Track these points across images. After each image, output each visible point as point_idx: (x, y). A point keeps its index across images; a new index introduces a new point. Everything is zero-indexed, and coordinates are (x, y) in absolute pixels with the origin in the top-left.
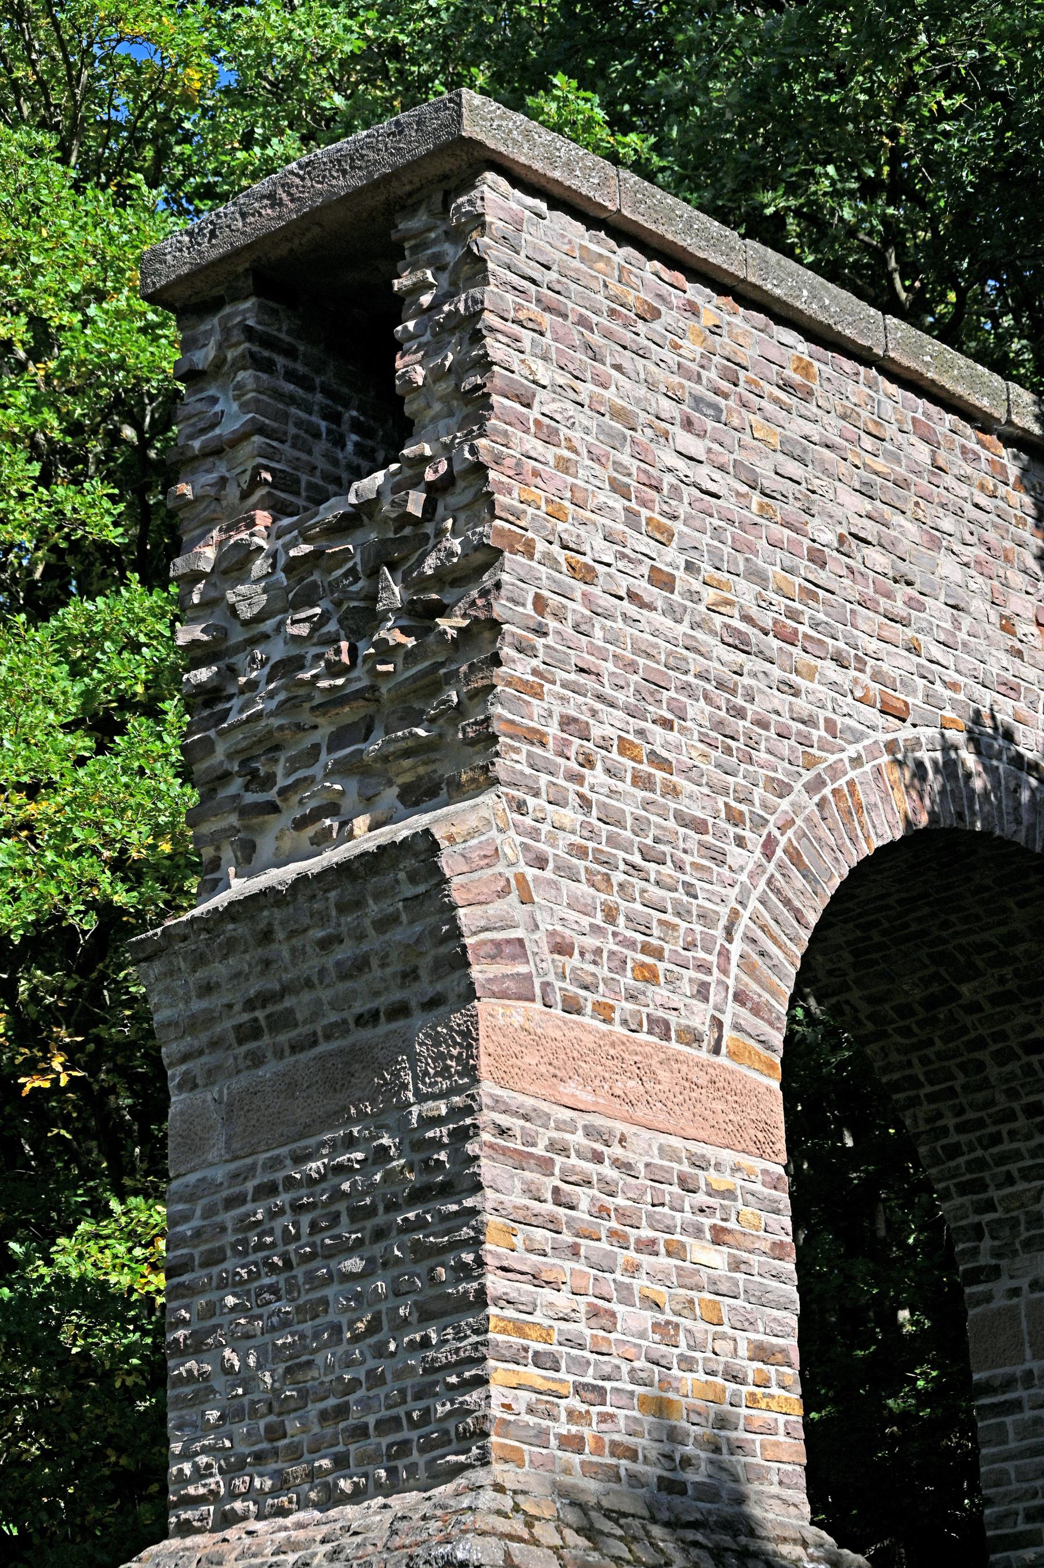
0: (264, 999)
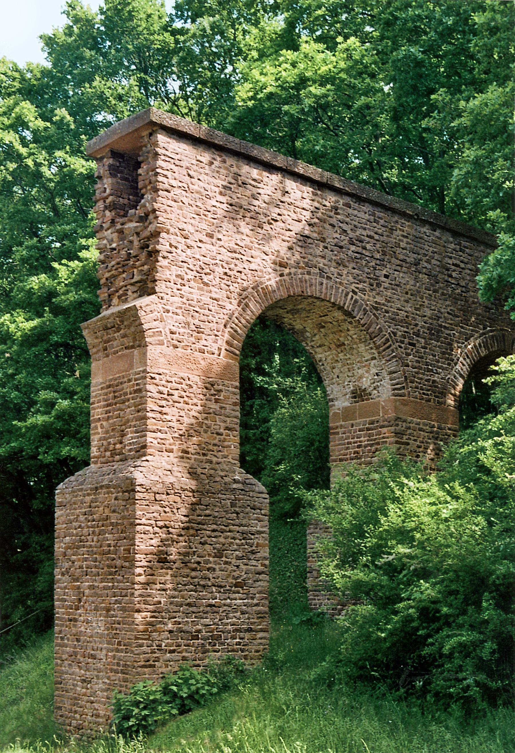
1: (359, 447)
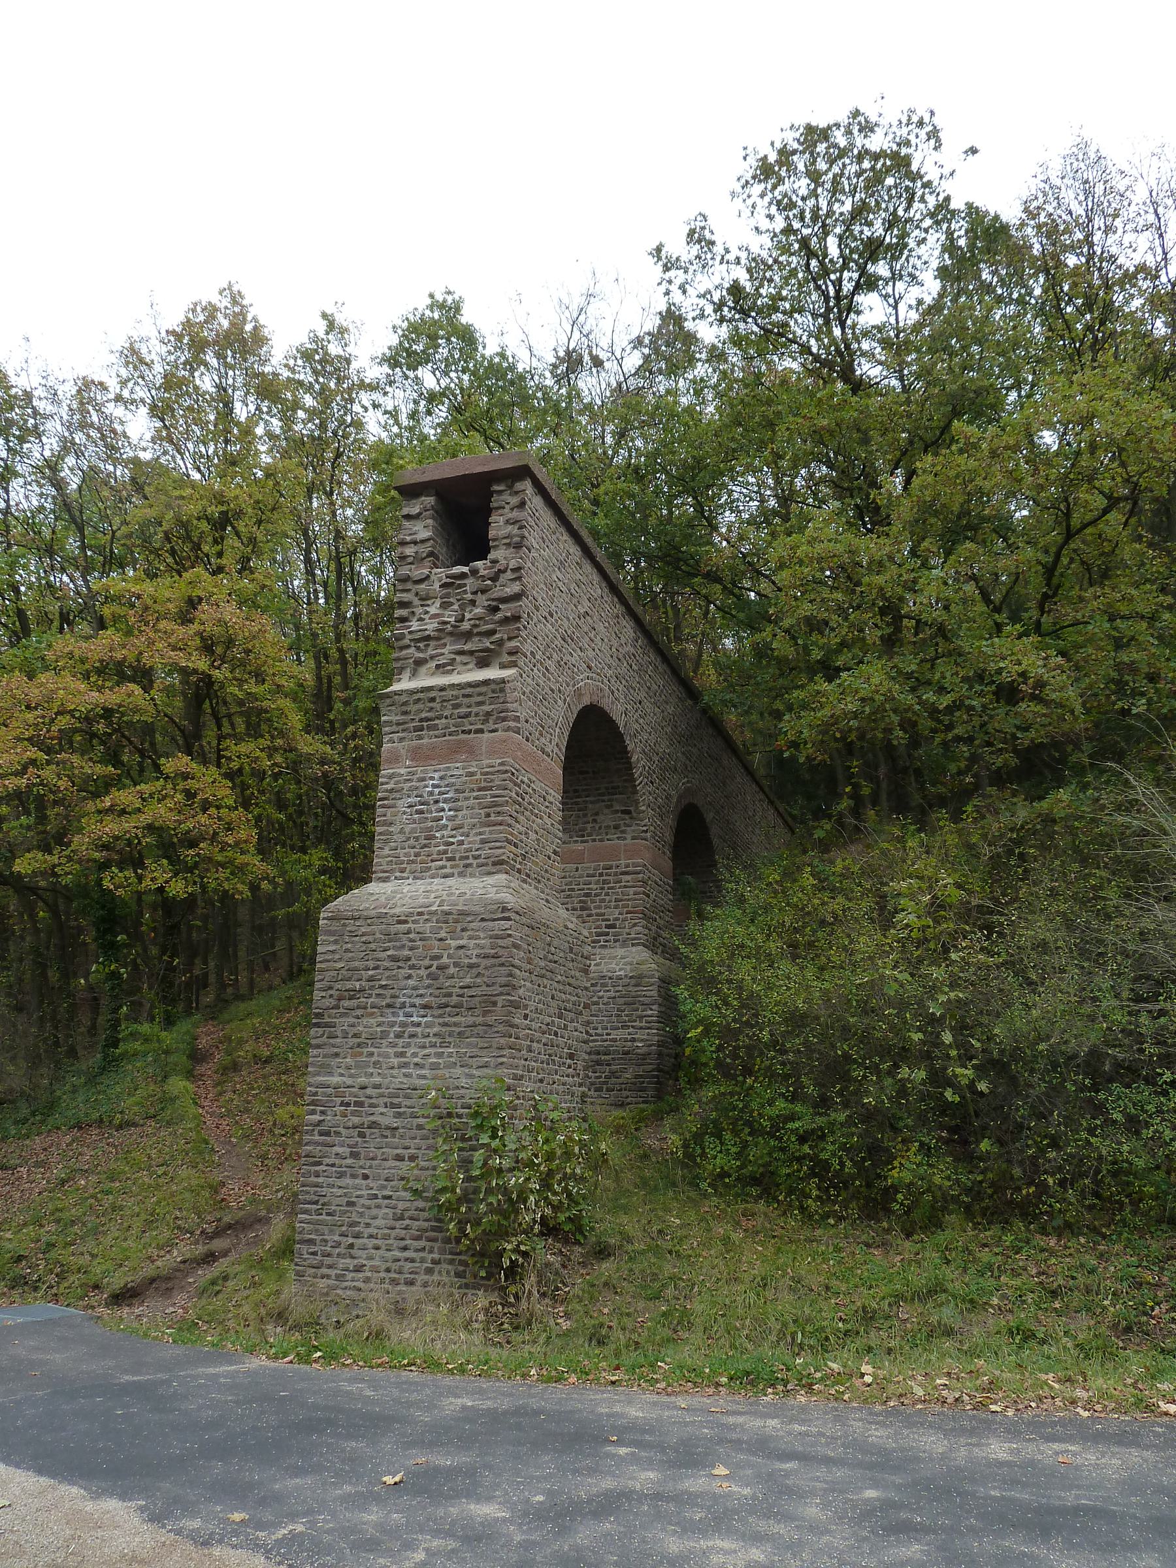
0: (427, 719)
1: (587, 895)
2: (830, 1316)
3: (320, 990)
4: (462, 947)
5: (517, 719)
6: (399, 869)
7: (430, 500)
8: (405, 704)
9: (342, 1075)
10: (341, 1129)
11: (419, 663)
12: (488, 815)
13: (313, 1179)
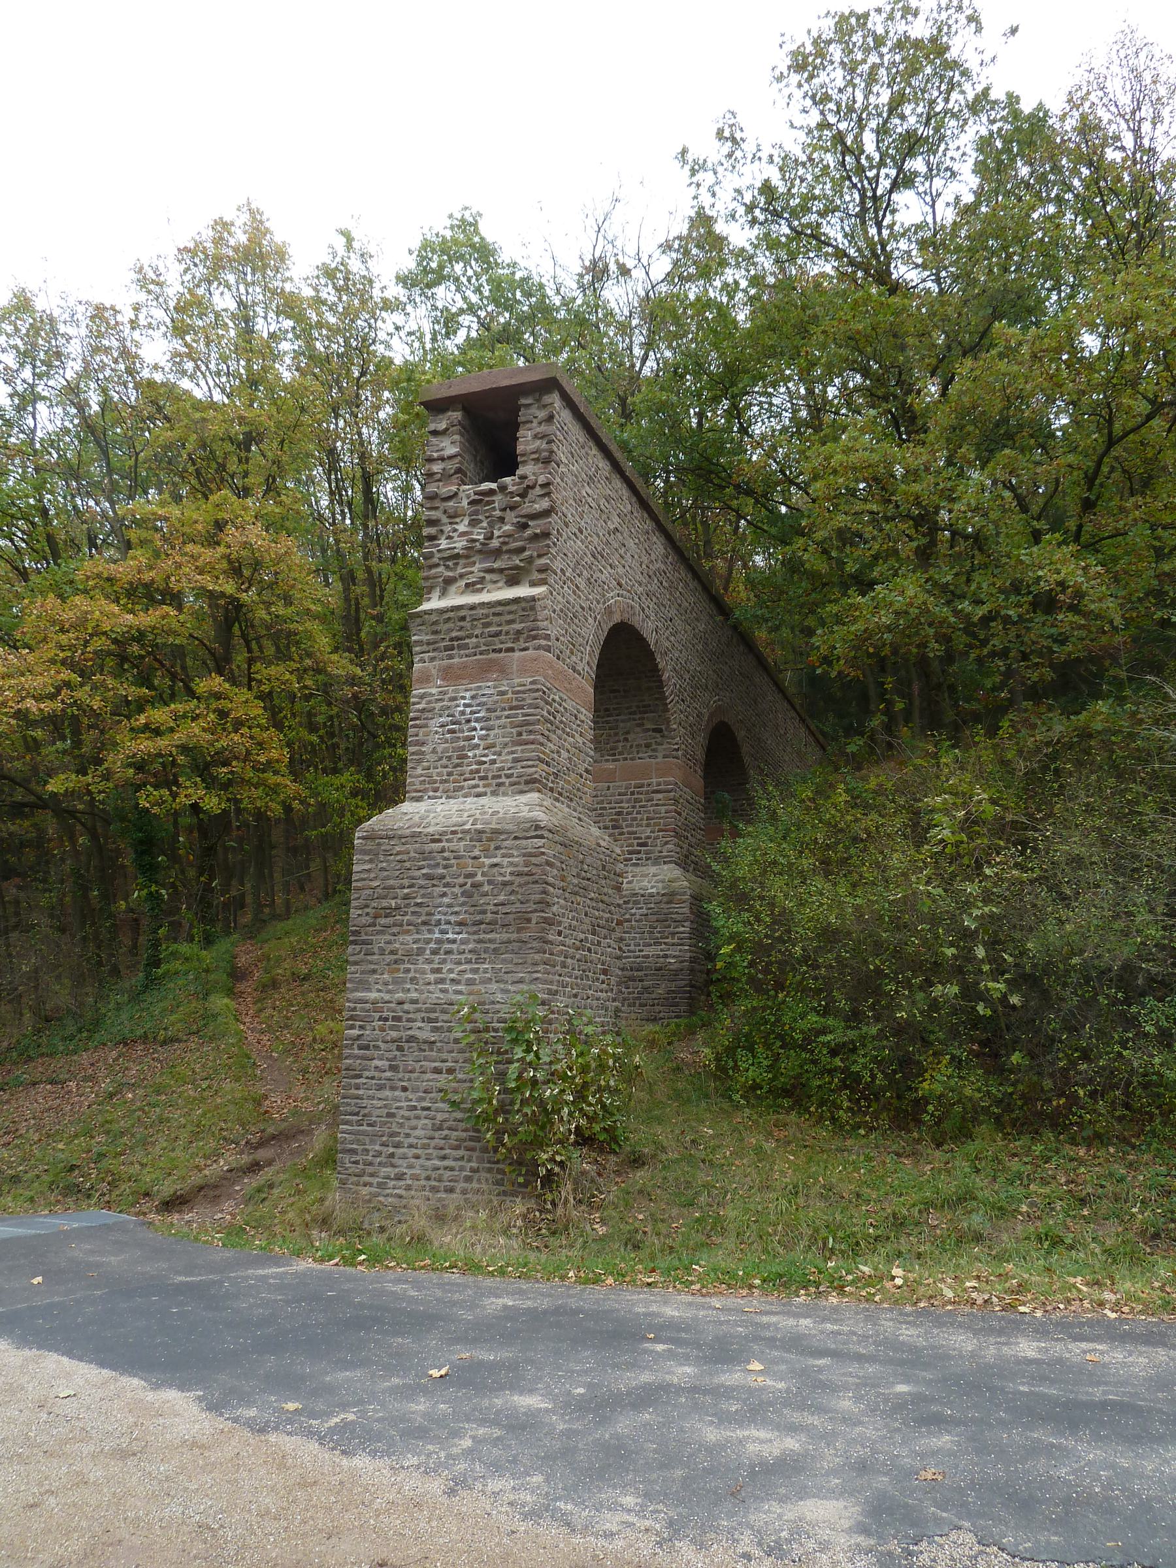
0: (458, 639)
1: (619, 813)
2: (864, 1222)
3: (356, 908)
4: (496, 865)
5: (547, 637)
6: (431, 789)
7: (456, 415)
8: (435, 623)
9: (379, 991)
10: (380, 1043)
11: (449, 582)
12: (520, 734)
13: (353, 1091)
